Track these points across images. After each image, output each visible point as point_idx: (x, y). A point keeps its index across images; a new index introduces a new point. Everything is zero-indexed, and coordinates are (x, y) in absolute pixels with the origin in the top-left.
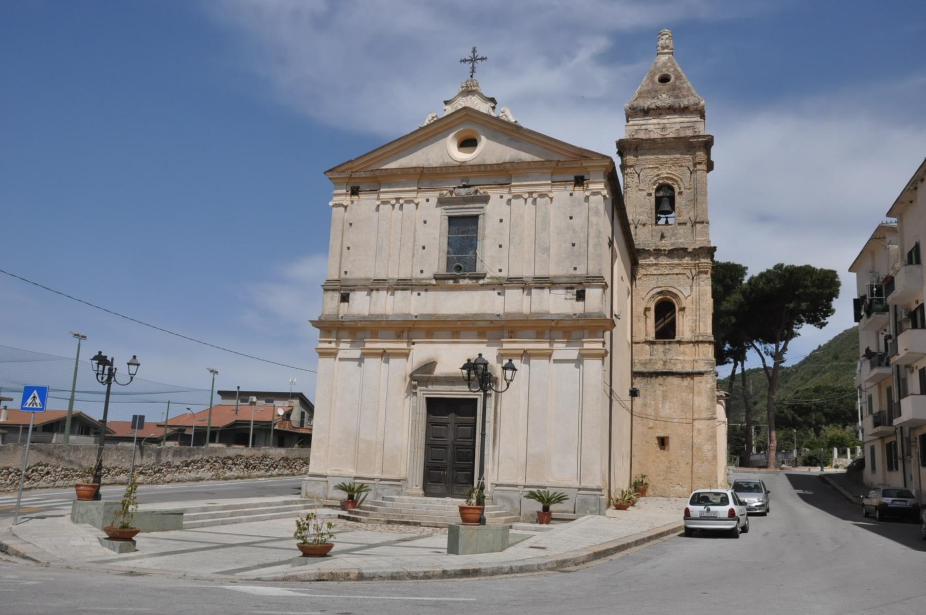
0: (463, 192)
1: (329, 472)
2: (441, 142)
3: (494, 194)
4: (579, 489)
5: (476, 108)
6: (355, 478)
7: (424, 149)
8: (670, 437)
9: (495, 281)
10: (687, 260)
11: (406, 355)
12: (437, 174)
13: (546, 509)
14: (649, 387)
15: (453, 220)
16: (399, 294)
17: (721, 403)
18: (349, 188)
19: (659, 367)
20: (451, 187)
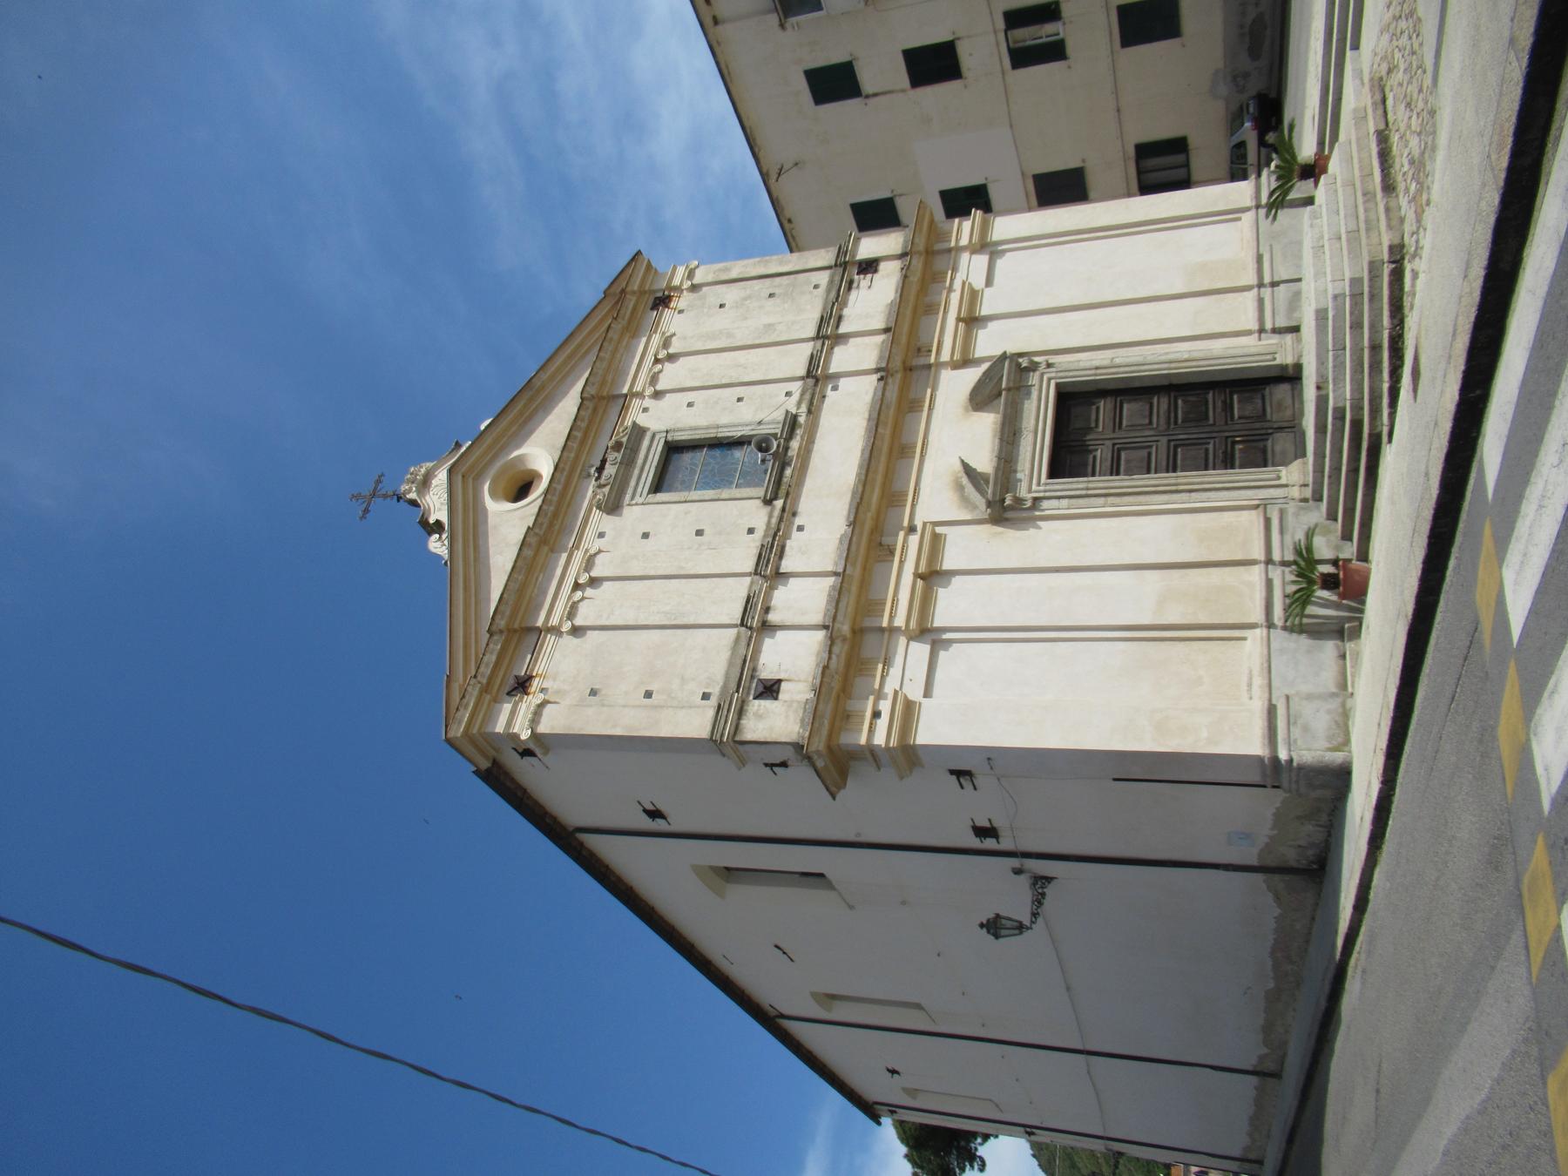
0: (610, 470)
1: (1258, 706)
2: (491, 520)
3: (635, 415)
6: (1270, 625)
7: (491, 551)
9: (808, 396)
12: (555, 515)
16: (787, 565)
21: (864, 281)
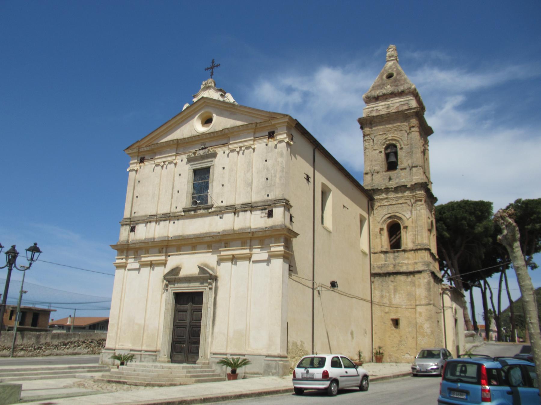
0: (202, 152)
1: (117, 347)
2: (191, 122)
3: (220, 151)
4: (266, 356)
5: (211, 97)
6: (131, 350)
8: (400, 318)
9: (218, 209)
10: (407, 193)
11: (164, 264)
12: (187, 143)
13: (234, 372)
14: (384, 283)
15: (196, 172)
16: (162, 223)
17: (447, 294)
18: (139, 159)
19: (391, 269)
20: (194, 150)
21: (265, 213)
